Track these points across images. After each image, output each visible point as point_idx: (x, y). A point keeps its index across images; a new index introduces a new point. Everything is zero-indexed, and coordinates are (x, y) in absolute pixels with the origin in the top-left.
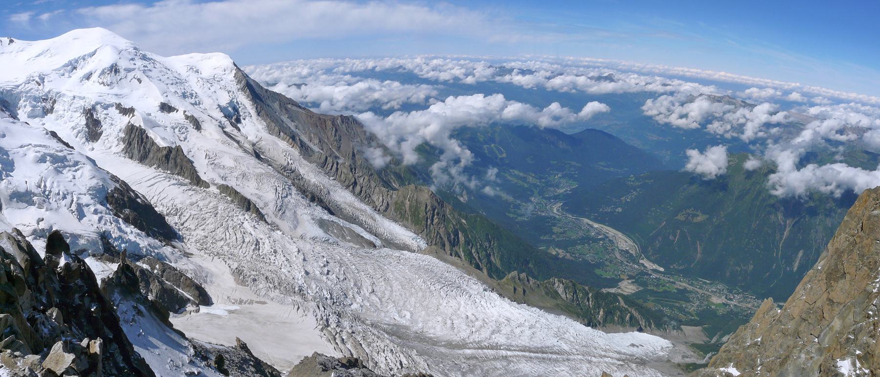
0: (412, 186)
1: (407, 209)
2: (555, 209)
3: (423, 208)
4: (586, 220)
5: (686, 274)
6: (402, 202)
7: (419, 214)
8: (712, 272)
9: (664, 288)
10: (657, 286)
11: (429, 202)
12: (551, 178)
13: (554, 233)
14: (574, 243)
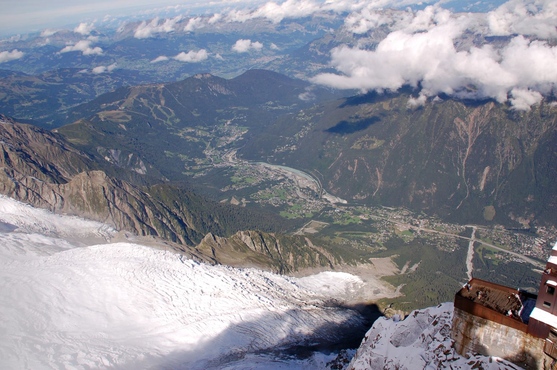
0: (84, 174)
1: (85, 199)
2: (230, 158)
3: (101, 193)
4: (263, 164)
5: (370, 203)
7: (99, 201)
8: (393, 198)
9: (350, 221)
10: (343, 218)
11: (105, 185)
12: (220, 128)
13: (234, 183)
14: (255, 189)
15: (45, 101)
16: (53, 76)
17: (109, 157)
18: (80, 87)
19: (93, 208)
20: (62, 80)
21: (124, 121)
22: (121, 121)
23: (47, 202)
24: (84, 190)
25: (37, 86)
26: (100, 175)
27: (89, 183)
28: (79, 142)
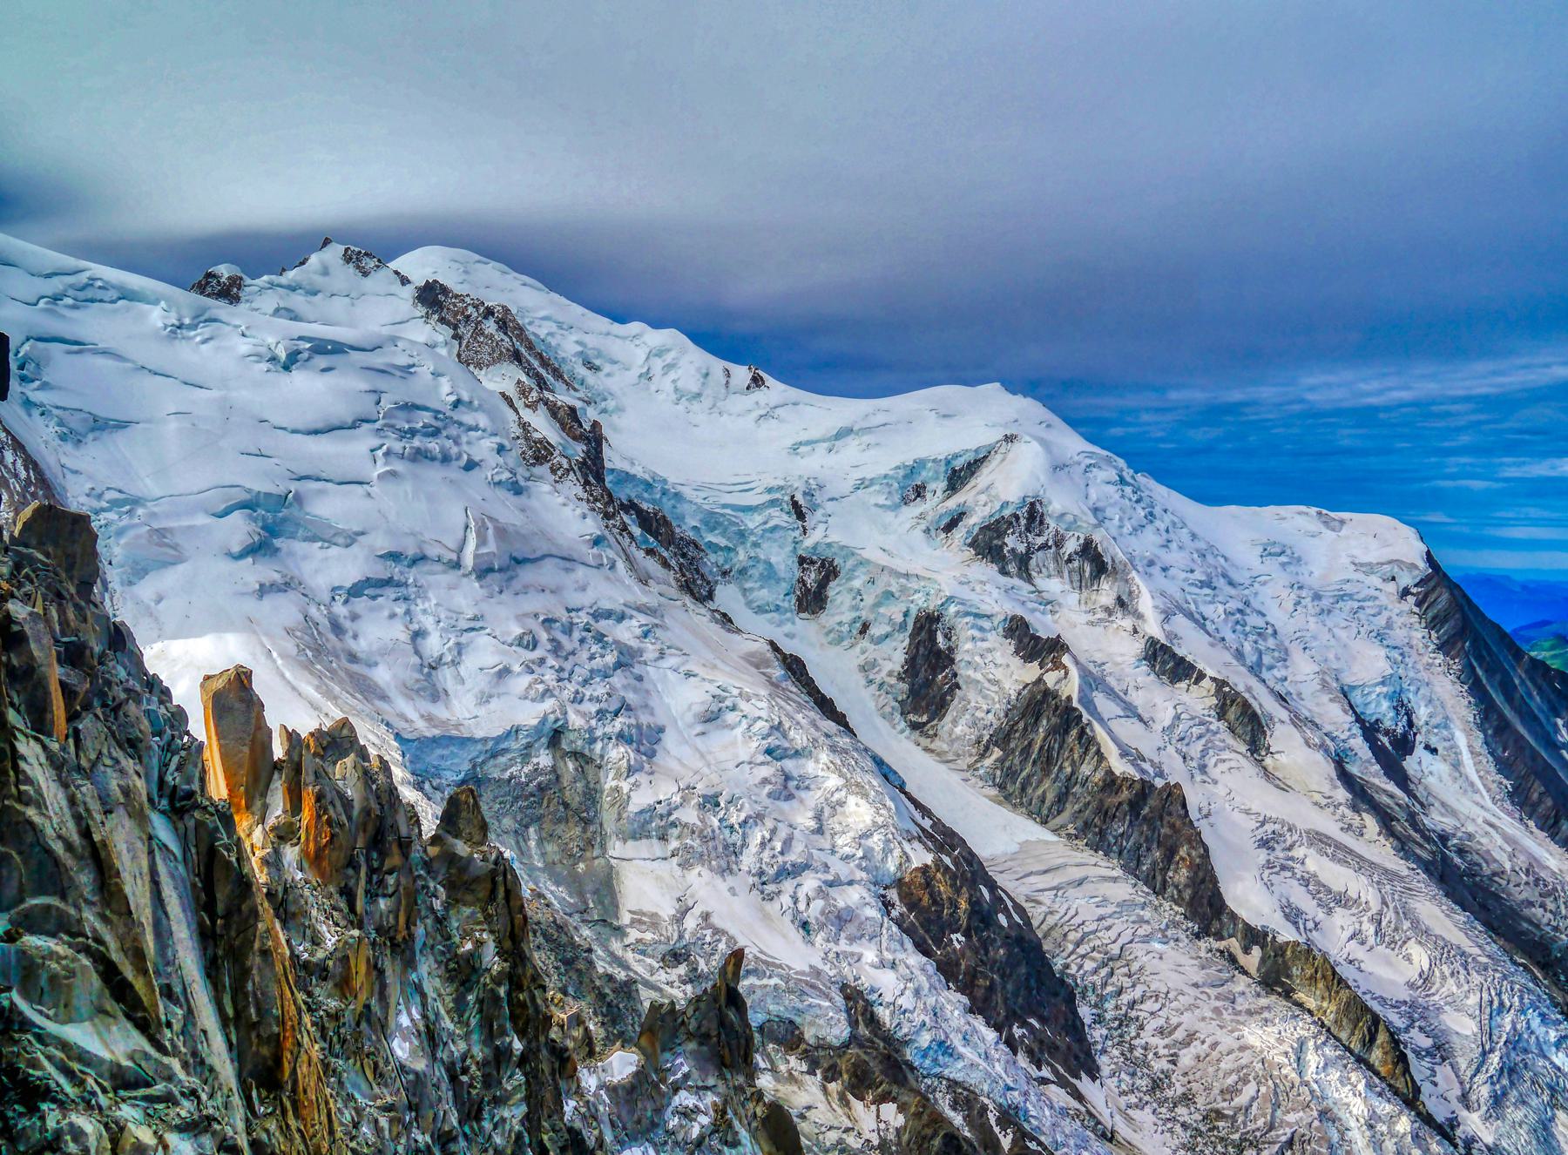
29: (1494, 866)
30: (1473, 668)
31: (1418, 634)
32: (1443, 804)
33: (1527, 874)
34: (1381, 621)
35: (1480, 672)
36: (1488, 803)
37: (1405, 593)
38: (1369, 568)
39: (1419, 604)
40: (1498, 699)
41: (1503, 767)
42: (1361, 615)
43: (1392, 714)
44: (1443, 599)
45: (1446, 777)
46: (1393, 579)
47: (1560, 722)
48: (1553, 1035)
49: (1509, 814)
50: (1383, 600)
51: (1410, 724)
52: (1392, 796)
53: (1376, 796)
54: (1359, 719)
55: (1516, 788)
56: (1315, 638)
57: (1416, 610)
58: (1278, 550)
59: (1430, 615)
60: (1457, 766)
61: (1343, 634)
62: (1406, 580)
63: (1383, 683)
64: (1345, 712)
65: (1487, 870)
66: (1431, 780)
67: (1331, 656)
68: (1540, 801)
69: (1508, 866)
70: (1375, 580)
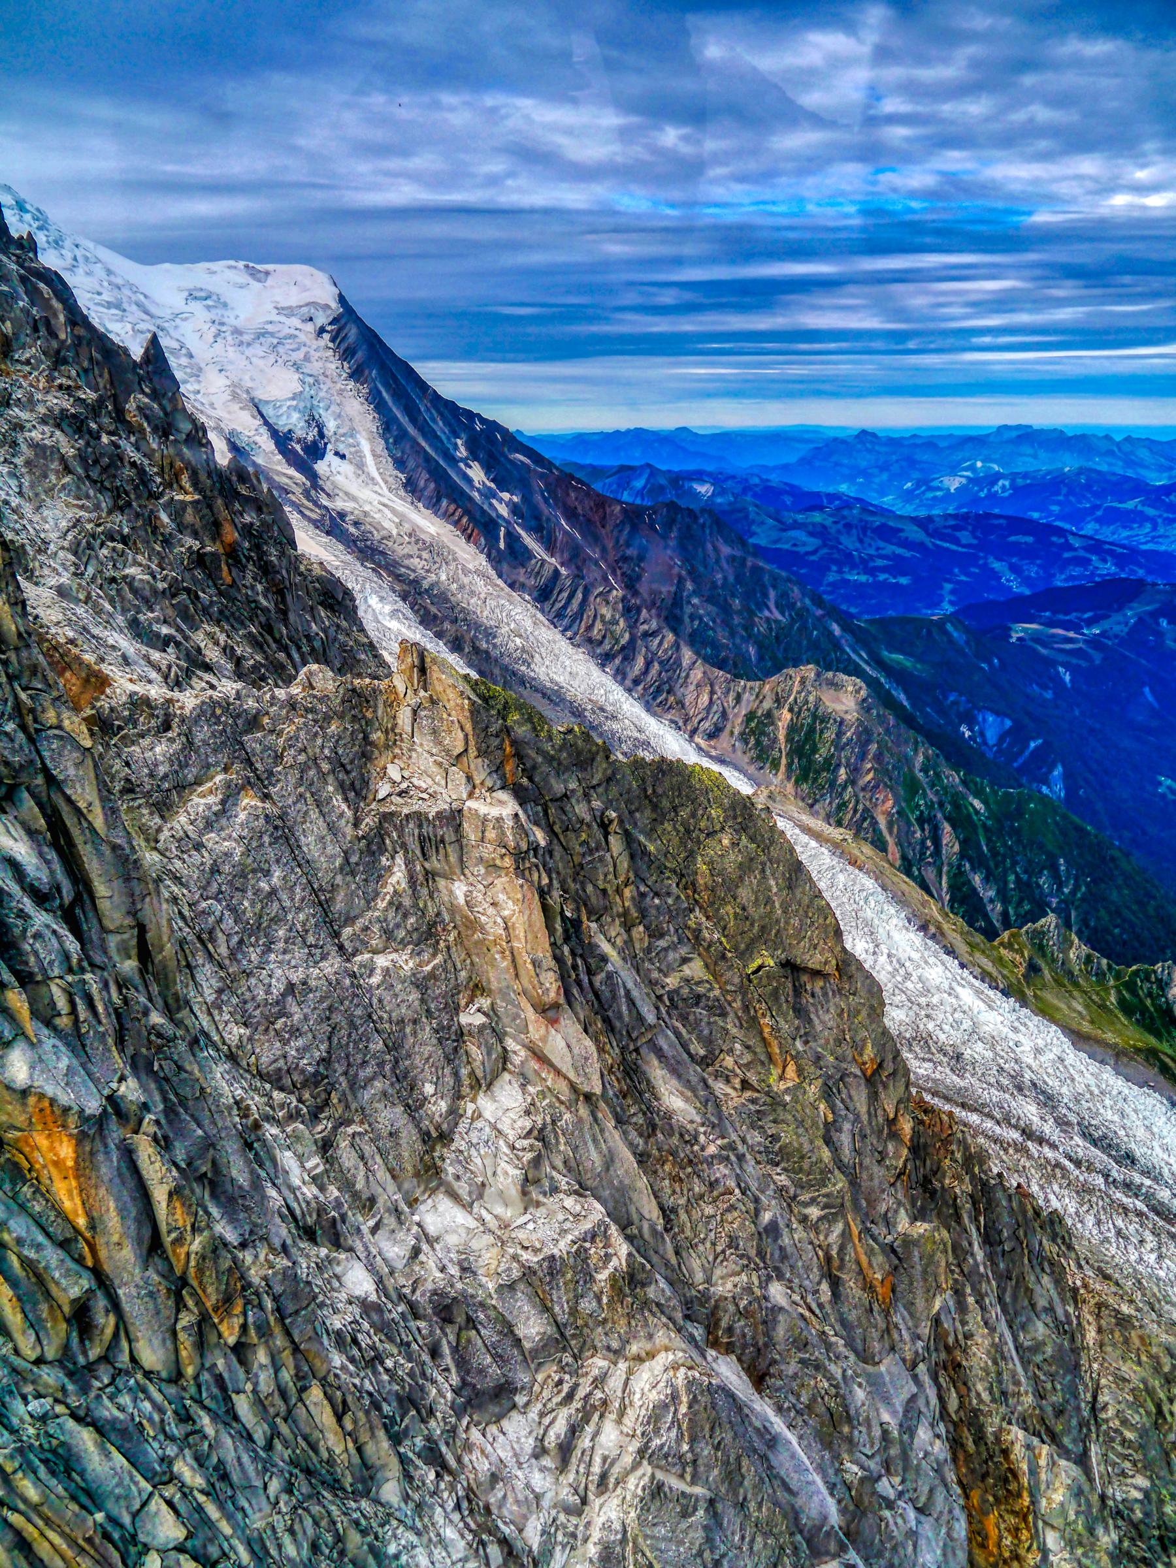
3: (830, 735)
6: (769, 714)
7: (815, 750)
15: (904, 581)
16: (956, 528)
17: (970, 729)
18: (1014, 569)
19: (789, 765)
20: (975, 542)
21: (1075, 661)
22: (1061, 658)
23: (683, 707)
24: (791, 710)
25: (907, 544)
26: (850, 688)
27: (811, 698)
28: (908, 664)
29: (384, 533)
30: (380, 393)
31: (333, 365)
32: (346, 494)
33: (410, 536)
34: (300, 355)
35: (385, 394)
36: (385, 491)
37: (322, 330)
38: (289, 311)
39: (333, 340)
40: (404, 420)
41: (400, 464)
42: (281, 349)
43: (302, 424)
44: (352, 332)
45: (351, 475)
46: (311, 319)
47: (459, 442)
48: (388, 609)
49: (401, 498)
50: (302, 337)
51: (321, 435)
52: (291, 478)
53: (276, 478)
54: (274, 433)
55: (409, 480)
56: (231, 362)
57: (331, 345)
58: (203, 294)
59: (343, 347)
60: (360, 466)
61: (261, 363)
62: (322, 319)
63: (293, 399)
64: (254, 417)
65: (377, 536)
66: (339, 479)
67: (247, 378)
68: (426, 487)
69: (394, 532)
70: (295, 322)
